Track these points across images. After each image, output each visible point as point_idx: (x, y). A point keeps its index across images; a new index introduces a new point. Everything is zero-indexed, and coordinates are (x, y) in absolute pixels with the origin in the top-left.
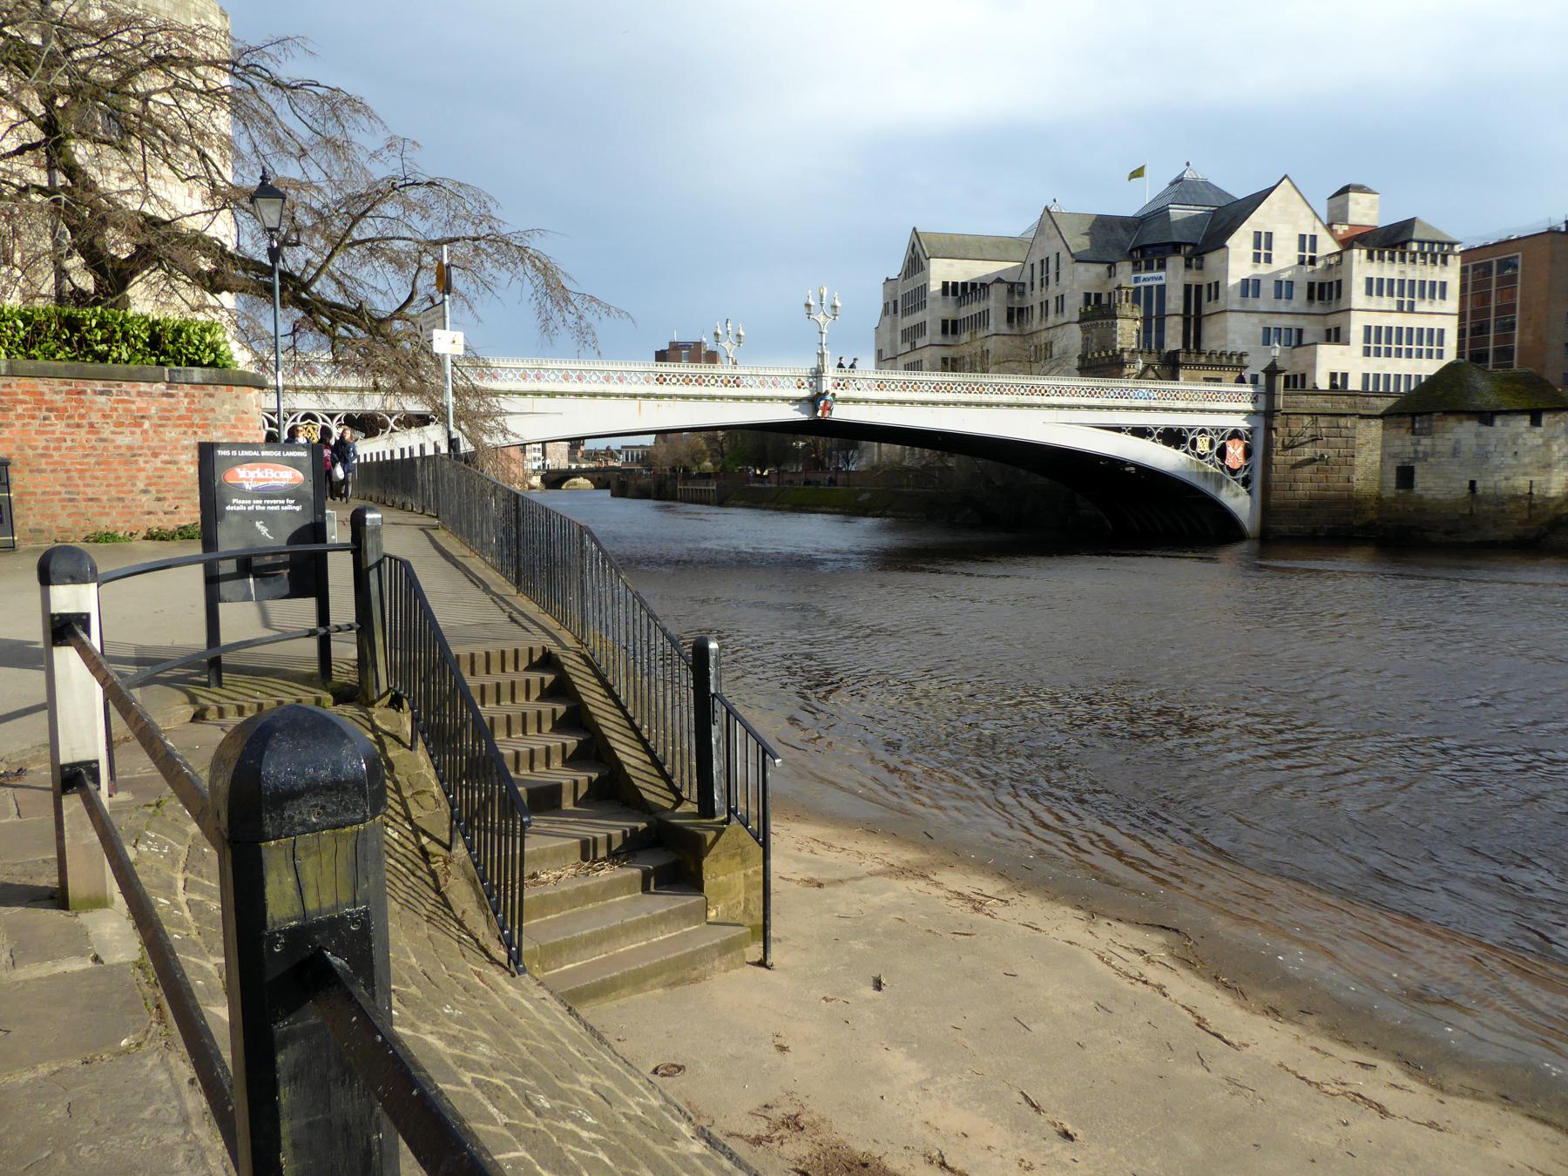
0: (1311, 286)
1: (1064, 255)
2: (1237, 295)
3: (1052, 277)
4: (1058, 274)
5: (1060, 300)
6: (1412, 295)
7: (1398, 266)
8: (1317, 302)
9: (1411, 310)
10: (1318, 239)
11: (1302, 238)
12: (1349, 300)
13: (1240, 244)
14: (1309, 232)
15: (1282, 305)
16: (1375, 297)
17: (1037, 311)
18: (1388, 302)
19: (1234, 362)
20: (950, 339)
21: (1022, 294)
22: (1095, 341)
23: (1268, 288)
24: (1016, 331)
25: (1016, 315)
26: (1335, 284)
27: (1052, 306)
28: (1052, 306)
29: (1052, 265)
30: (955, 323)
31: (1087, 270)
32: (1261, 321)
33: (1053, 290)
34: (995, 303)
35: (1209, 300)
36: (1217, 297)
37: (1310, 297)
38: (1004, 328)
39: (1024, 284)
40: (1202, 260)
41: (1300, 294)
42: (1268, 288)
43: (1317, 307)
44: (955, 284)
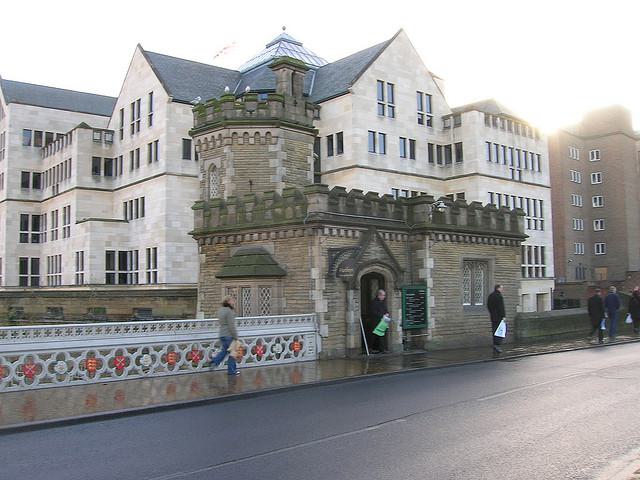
0: (430, 146)
1: (161, 94)
2: (365, 149)
3: (144, 120)
5: (154, 147)
9: (520, 181)
13: (366, 89)
15: (408, 166)
16: (494, 166)
17: (127, 163)
19: (508, 228)
20: (32, 194)
21: (111, 143)
22: (230, 171)
23: (393, 143)
24: (103, 184)
25: (104, 168)
27: (144, 155)
28: (144, 155)
29: (144, 108)
30: (37, 176)
32: (391, 181)
33: (146, 135)
34: (76, 153)
35: (330, 154)
36: (341, 149)
37: (431, 160)
38: (89, 181)
39: (112, 132)
40: (319, 108)
41: (422, 153)
42: (393, 143)
43: (437, 172)
44: (39, 134)
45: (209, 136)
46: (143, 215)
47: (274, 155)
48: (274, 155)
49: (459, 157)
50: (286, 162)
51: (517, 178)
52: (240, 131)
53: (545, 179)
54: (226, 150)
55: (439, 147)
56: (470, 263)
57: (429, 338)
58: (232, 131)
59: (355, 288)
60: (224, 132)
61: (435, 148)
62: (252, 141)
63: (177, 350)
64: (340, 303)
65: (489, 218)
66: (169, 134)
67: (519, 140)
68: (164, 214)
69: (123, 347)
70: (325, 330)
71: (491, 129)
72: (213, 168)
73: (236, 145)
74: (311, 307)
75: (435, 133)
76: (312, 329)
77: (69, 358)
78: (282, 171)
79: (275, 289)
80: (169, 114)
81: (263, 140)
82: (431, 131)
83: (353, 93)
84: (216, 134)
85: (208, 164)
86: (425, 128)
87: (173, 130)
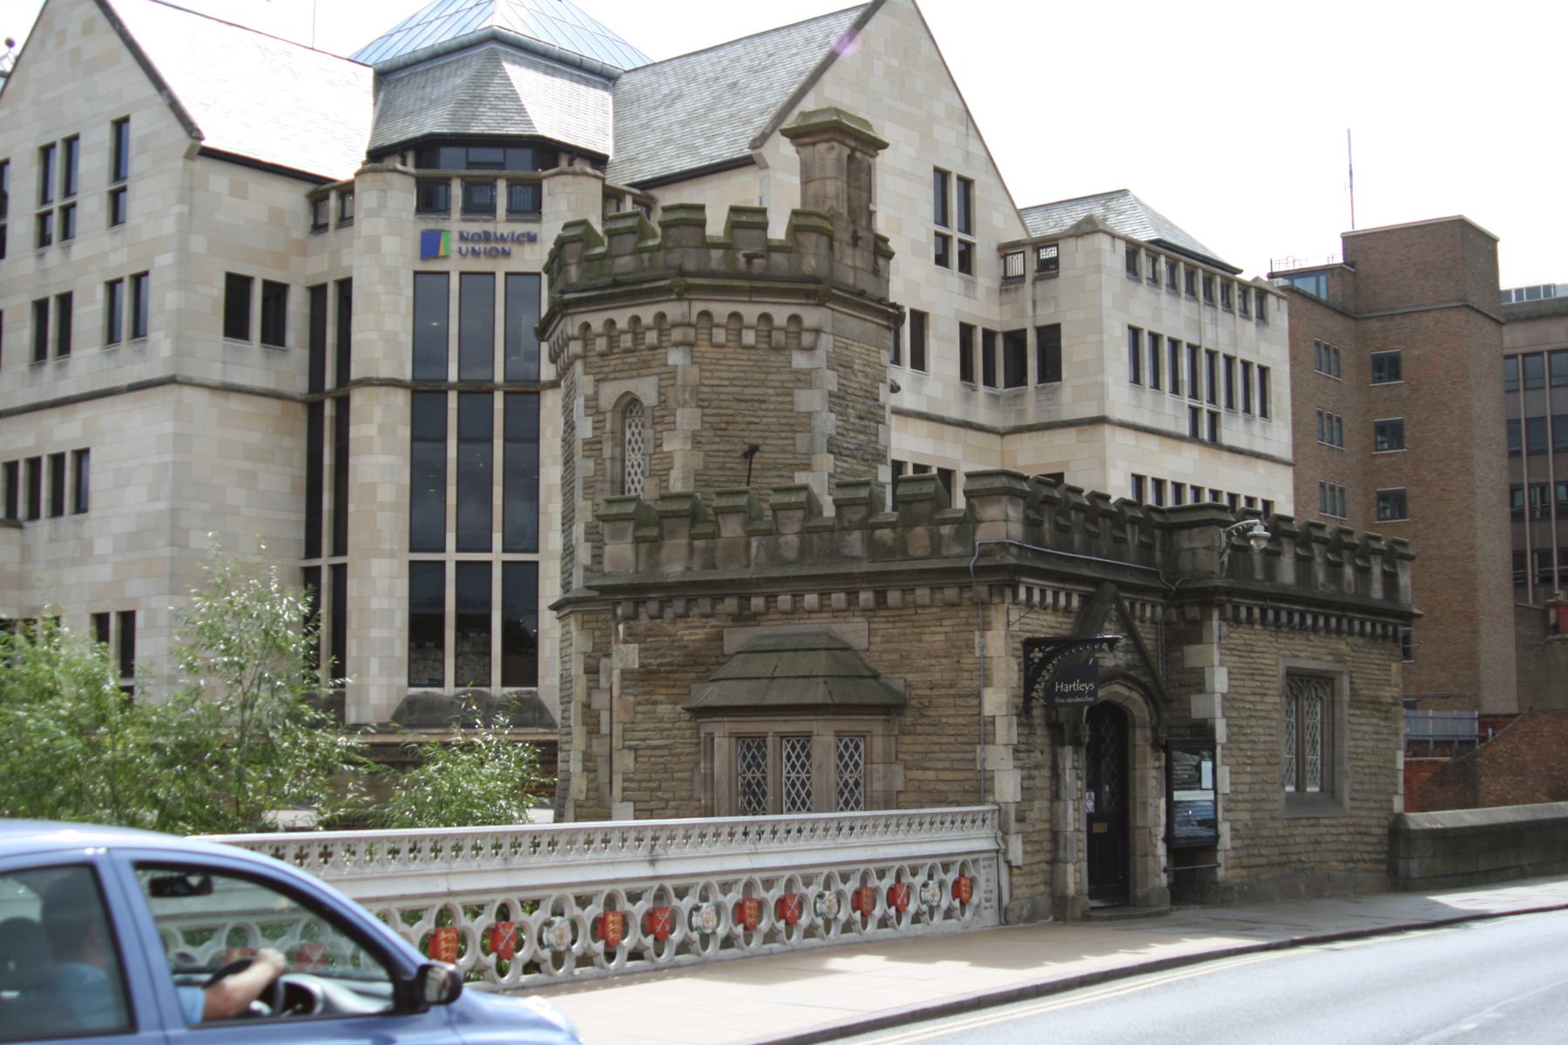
0: (966, 330)
4: (116, 197)
6: (1213, 399)
7: (1184, 306)
8: (982, 389)
9: (1214, 441)
10: (978, 193)
11: (942, 176)
12: (1101, 392)
14: (956, 168)
18: (1172, 412)
22: (687, 418)
26: (1031, 340)
27: (88, 317)
31: (238, 192)
37: (966, 373)
45: (622, 318)
46: (81, 507)
47: (805, 379)
48: (805, 379)
49: (1051, 370)
50: (837, 400)
51: (1204, 433)
52: (721, 310)
53: (1278, 436)
54: (676, 357)
55: (989, 335)
56: (1300, 683)
57: (1221, 873)
58: (698, 307)
59: (1076, 743)
60: (674, 310)
61: (978, 338)
62: (749, 337)
63: (624, 905)
64: (1042, 778)
65: (1340, 565)
66: (185, 258)
67: (1215, 322)
68: (162, 505)
69: (757, 877)
70: (1016, 850)
71: (1143, 290)
72: (629, 405)
73: (703, 347)
74: (979, 789)
75: (981, 292)
76: (993, 846)
77: (573, 911)
78: (828, 422)
79: (878, 744)
80: (188, 193)
81: (778, 337)
82: (970, 288)
83: (765, 166)
84: (647, 314)
85: (610, 393)
86: (953, 276)
87: (198, 244)
